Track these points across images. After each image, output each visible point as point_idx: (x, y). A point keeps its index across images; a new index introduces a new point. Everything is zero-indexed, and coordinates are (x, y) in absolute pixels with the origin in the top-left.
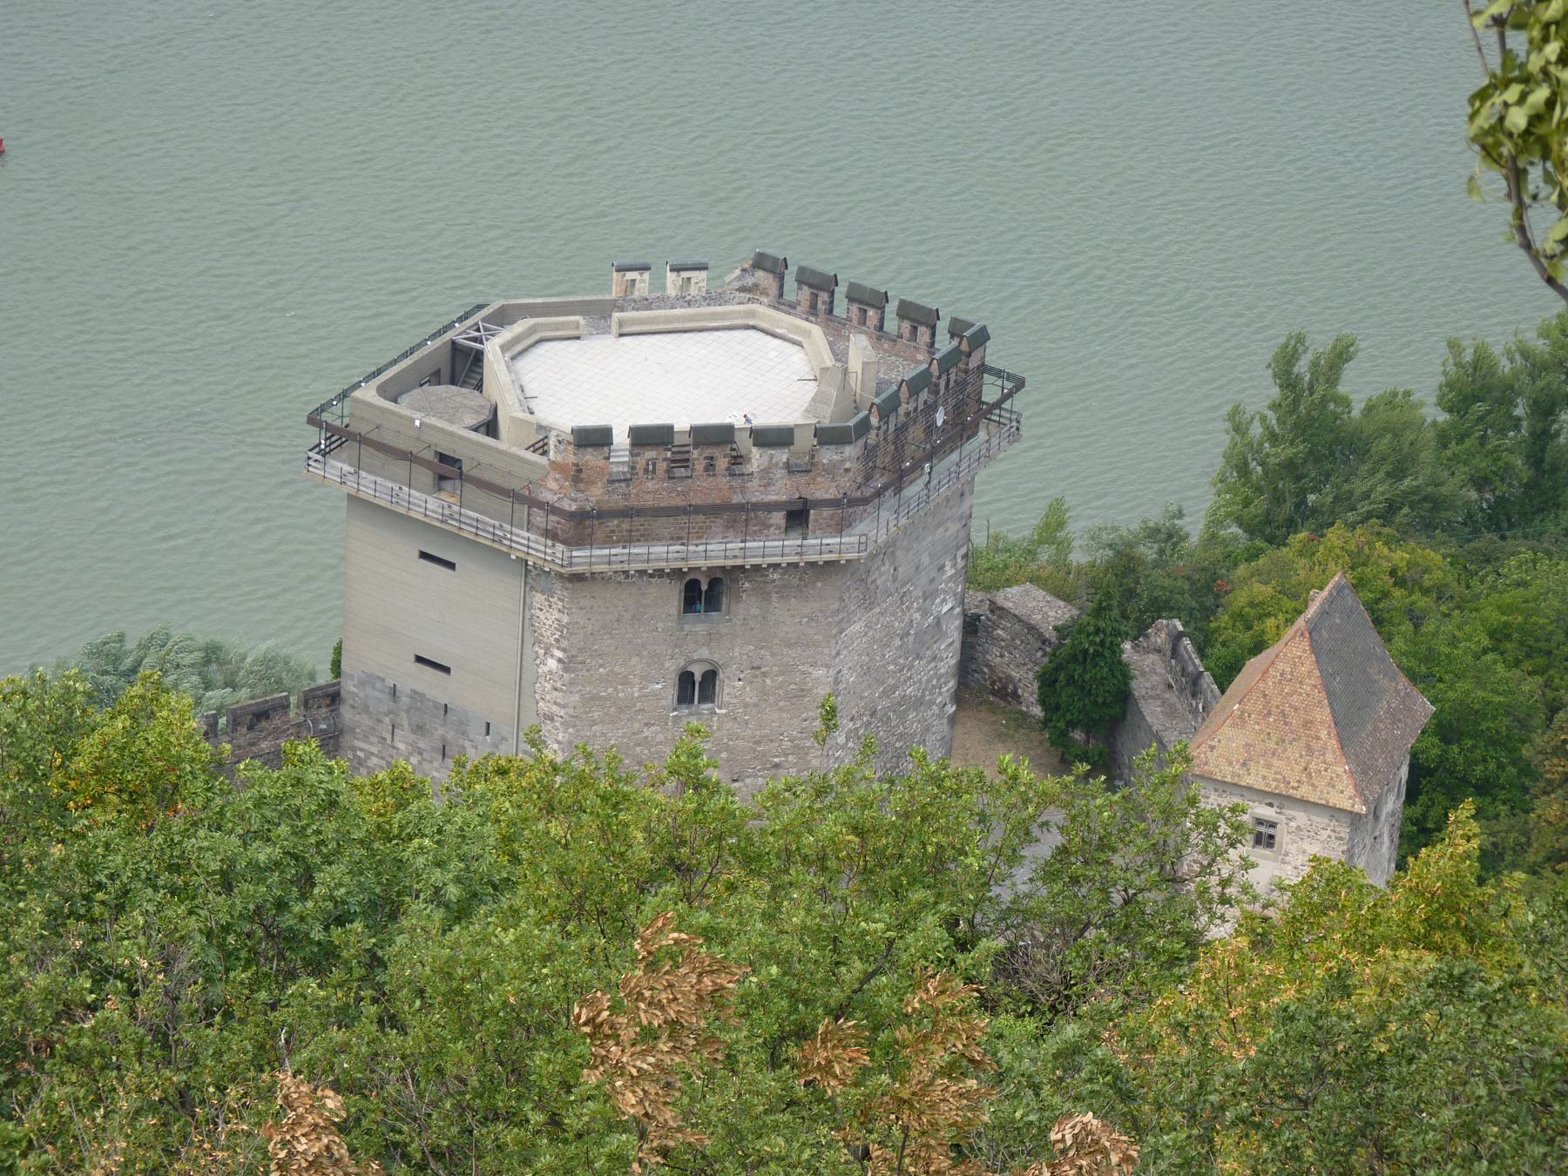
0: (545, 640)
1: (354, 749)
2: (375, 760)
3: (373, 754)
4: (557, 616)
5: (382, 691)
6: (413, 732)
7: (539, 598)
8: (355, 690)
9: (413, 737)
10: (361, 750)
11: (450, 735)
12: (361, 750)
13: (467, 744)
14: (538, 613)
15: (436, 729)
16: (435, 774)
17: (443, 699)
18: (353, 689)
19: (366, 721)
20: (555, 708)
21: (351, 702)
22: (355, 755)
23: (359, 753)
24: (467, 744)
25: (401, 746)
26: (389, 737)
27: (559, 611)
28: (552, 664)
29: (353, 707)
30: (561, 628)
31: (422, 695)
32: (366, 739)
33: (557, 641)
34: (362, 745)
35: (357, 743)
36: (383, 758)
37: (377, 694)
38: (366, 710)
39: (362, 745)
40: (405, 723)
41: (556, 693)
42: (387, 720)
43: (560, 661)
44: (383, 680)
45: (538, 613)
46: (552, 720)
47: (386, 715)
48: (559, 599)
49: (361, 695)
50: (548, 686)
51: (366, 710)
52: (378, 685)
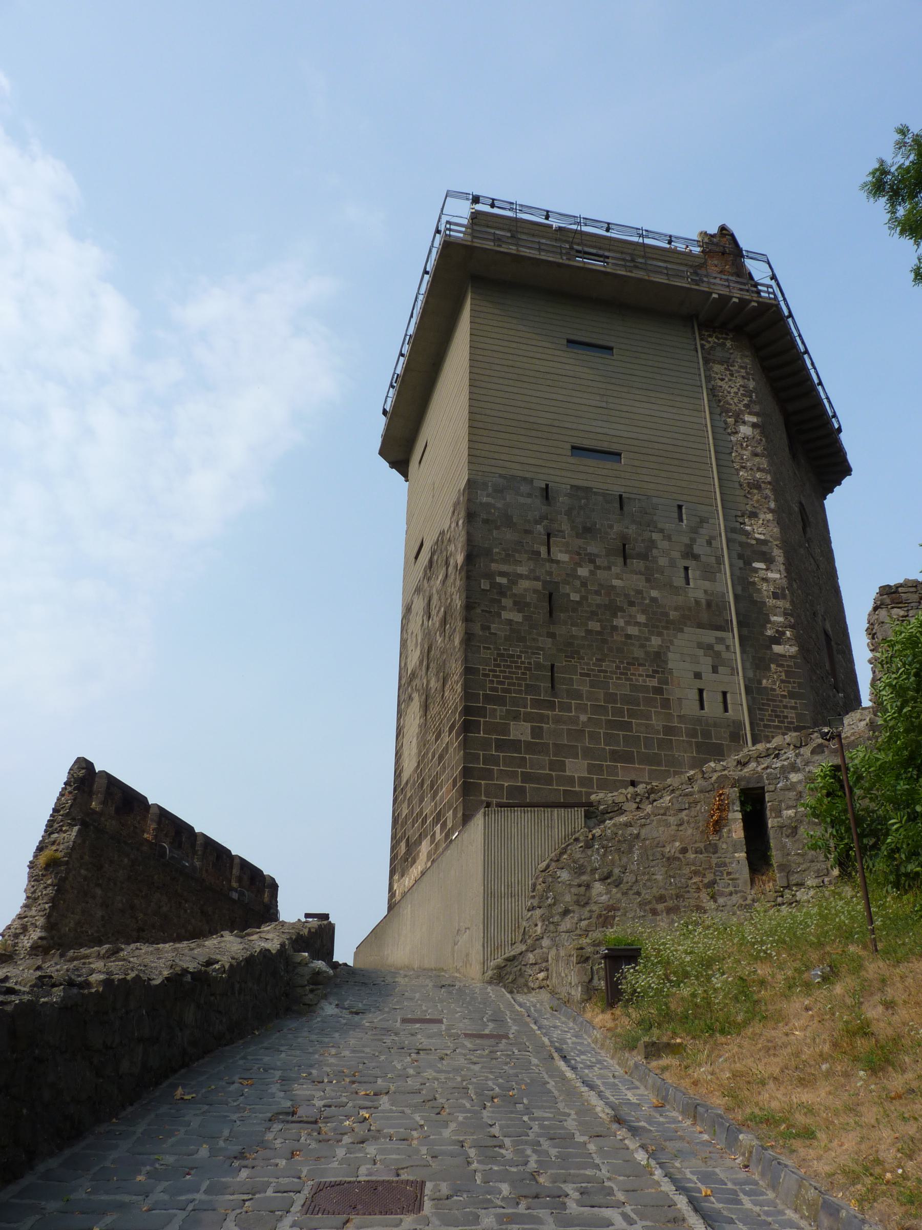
0: (733, 407)
1: (490, 576)
2: (524, 584)
3: (521, 576)
4: (741, 383)
5: (529, 495)
6: (578, 536)
7: (717, 368)
8: (490, 500)
9: (580, 542)
10: (502, 574)
11: (632, 530)
12: (502, 574)
13: (655, 536)
14: (720, 383)
15: (611, 527)
16: (616, 582)
17: (616, 489)
18: (485, 500)
19: (509, 535)
20: (758, 475)
21: (484, 516)
22: (493, 585)
23: (499, 579)
24: (655, 536)
25: (563, 557)
26: (543, 550)
27: (743, 377)
28: (745, 430)
29: (486, 521)
30: (748, 393)
31: (588, 490)
32: (508, 558)
33: (746, 406)
34: (504, 568)
35: (494, 566)
36: (537, 579)
37: (529, 501)
38: (508, 522)
39: (504, 568)
40: (566, 527)
41: (757, 459)
42: (540, 528)
43: (754, 426)
44: (531, 481)
45: (720, 383)
46: (758, 487)
47: (537, 522)
48: (741, 367)
49: (499, 505)
50: (746, 454)
51: (508, 522)
52: (524, 488)
